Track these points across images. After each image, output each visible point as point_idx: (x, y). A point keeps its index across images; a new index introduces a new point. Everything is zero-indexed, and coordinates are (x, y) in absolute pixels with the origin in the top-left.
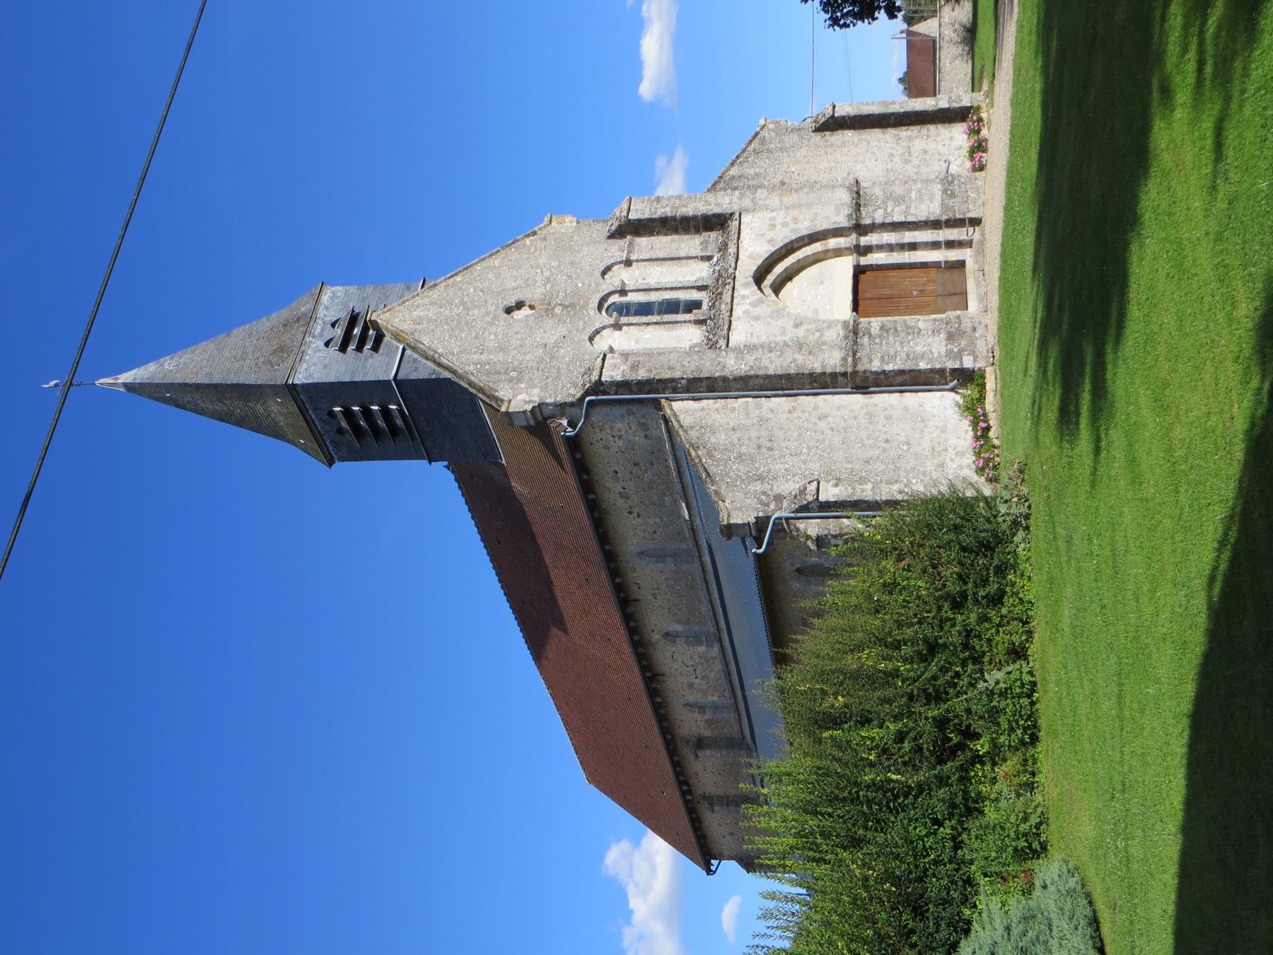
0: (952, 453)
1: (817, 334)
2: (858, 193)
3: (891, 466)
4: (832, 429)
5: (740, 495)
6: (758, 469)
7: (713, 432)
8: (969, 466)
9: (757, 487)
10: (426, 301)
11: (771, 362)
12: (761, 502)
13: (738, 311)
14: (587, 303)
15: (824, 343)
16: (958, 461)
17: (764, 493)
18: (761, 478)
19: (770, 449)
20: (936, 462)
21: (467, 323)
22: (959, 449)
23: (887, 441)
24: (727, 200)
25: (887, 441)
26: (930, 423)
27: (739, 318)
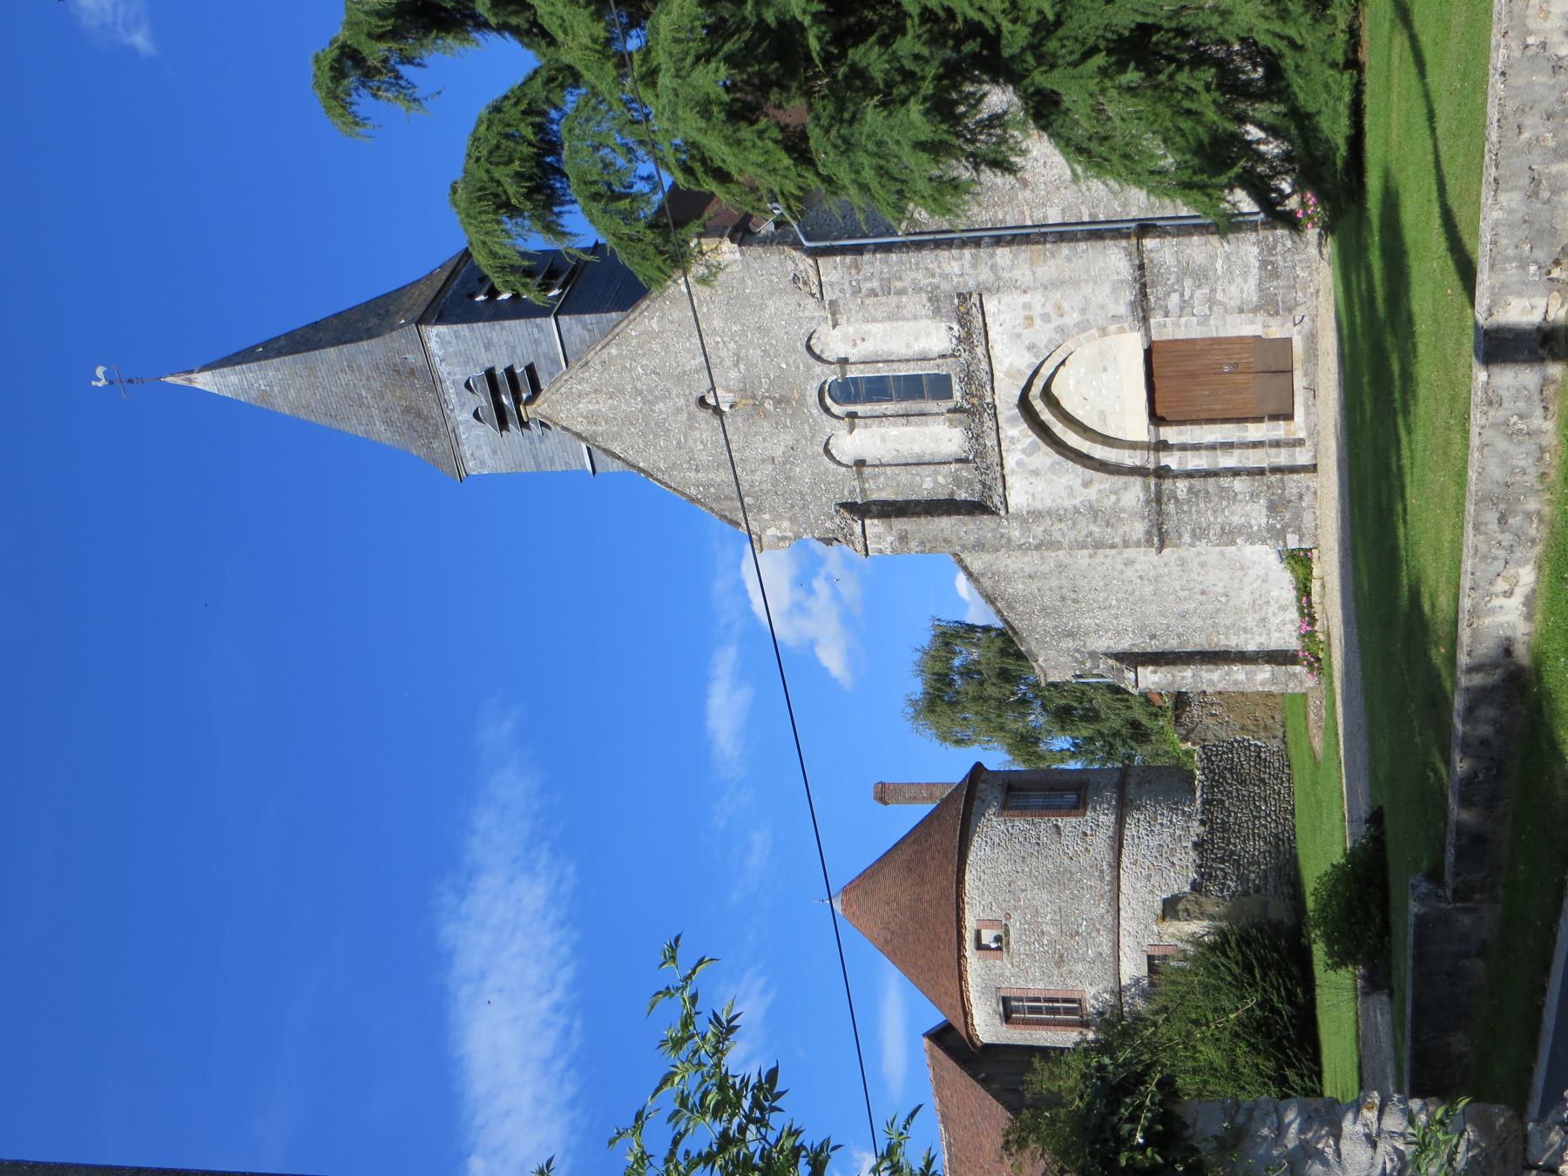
0: (1274, 607)
1: (1113, 498)
2: (1141, 267)
3: (1210, 622)
4: (1141, 577)
5: (1052, 653)
6: (1066, 625)
7: (1008, 580)
8: (1292, 621)
9: (1069, 644)
10: (587, 387)
11: (1063, 535)
12: (1077, 661)
13: (1010, 462)
14: (803, 396)
15: (1123, 510)
16: (1282, 616)
17: (1077, 651)
18: (1071, 634)
19: (1075, 601)
20: (1257, 616)
21: (657, 424)
22: (1283, 602)
23: (1203, 592)
24: (955, 267)
25: (1203, 592)
26: (1250, 572)
27: (1013, 472)
